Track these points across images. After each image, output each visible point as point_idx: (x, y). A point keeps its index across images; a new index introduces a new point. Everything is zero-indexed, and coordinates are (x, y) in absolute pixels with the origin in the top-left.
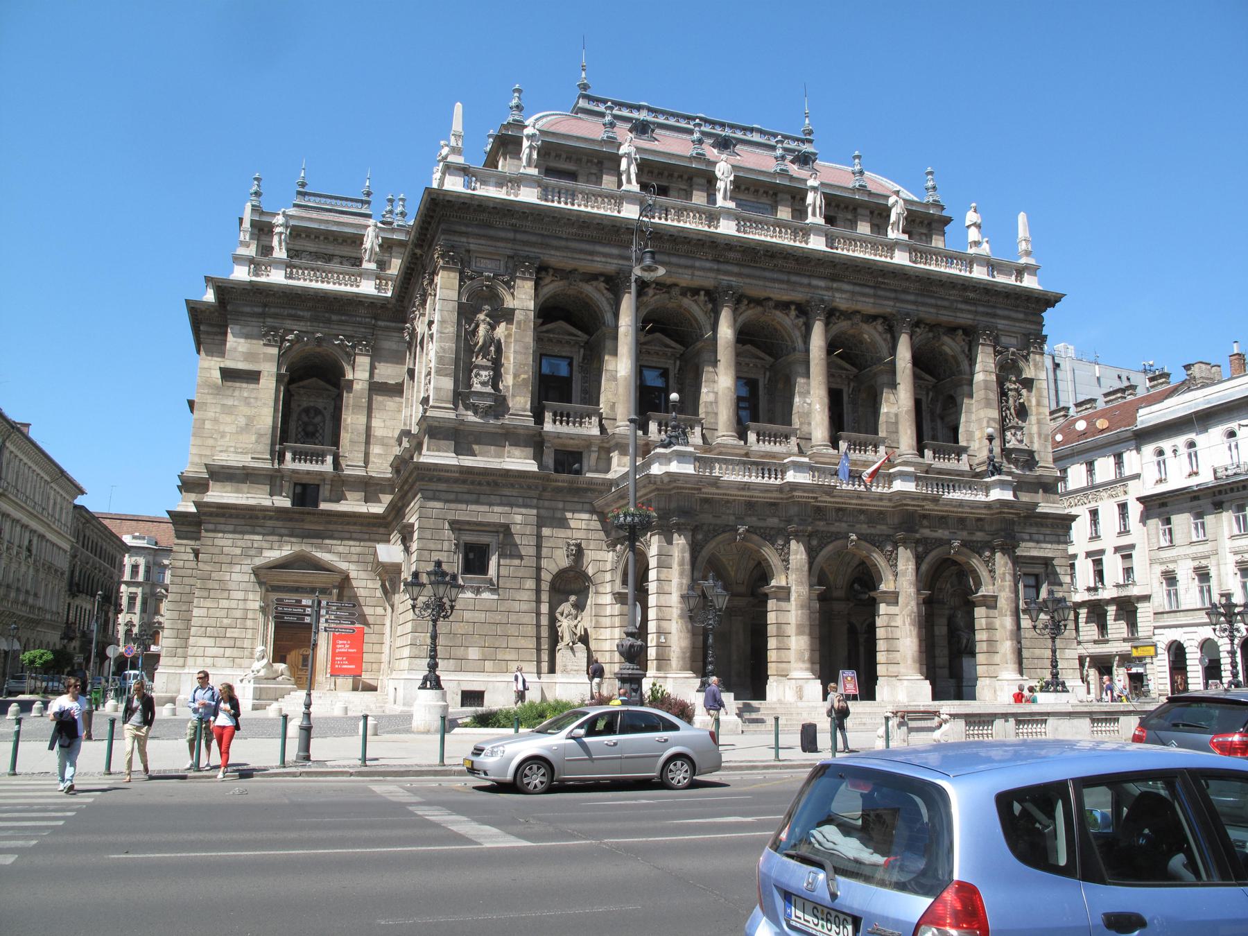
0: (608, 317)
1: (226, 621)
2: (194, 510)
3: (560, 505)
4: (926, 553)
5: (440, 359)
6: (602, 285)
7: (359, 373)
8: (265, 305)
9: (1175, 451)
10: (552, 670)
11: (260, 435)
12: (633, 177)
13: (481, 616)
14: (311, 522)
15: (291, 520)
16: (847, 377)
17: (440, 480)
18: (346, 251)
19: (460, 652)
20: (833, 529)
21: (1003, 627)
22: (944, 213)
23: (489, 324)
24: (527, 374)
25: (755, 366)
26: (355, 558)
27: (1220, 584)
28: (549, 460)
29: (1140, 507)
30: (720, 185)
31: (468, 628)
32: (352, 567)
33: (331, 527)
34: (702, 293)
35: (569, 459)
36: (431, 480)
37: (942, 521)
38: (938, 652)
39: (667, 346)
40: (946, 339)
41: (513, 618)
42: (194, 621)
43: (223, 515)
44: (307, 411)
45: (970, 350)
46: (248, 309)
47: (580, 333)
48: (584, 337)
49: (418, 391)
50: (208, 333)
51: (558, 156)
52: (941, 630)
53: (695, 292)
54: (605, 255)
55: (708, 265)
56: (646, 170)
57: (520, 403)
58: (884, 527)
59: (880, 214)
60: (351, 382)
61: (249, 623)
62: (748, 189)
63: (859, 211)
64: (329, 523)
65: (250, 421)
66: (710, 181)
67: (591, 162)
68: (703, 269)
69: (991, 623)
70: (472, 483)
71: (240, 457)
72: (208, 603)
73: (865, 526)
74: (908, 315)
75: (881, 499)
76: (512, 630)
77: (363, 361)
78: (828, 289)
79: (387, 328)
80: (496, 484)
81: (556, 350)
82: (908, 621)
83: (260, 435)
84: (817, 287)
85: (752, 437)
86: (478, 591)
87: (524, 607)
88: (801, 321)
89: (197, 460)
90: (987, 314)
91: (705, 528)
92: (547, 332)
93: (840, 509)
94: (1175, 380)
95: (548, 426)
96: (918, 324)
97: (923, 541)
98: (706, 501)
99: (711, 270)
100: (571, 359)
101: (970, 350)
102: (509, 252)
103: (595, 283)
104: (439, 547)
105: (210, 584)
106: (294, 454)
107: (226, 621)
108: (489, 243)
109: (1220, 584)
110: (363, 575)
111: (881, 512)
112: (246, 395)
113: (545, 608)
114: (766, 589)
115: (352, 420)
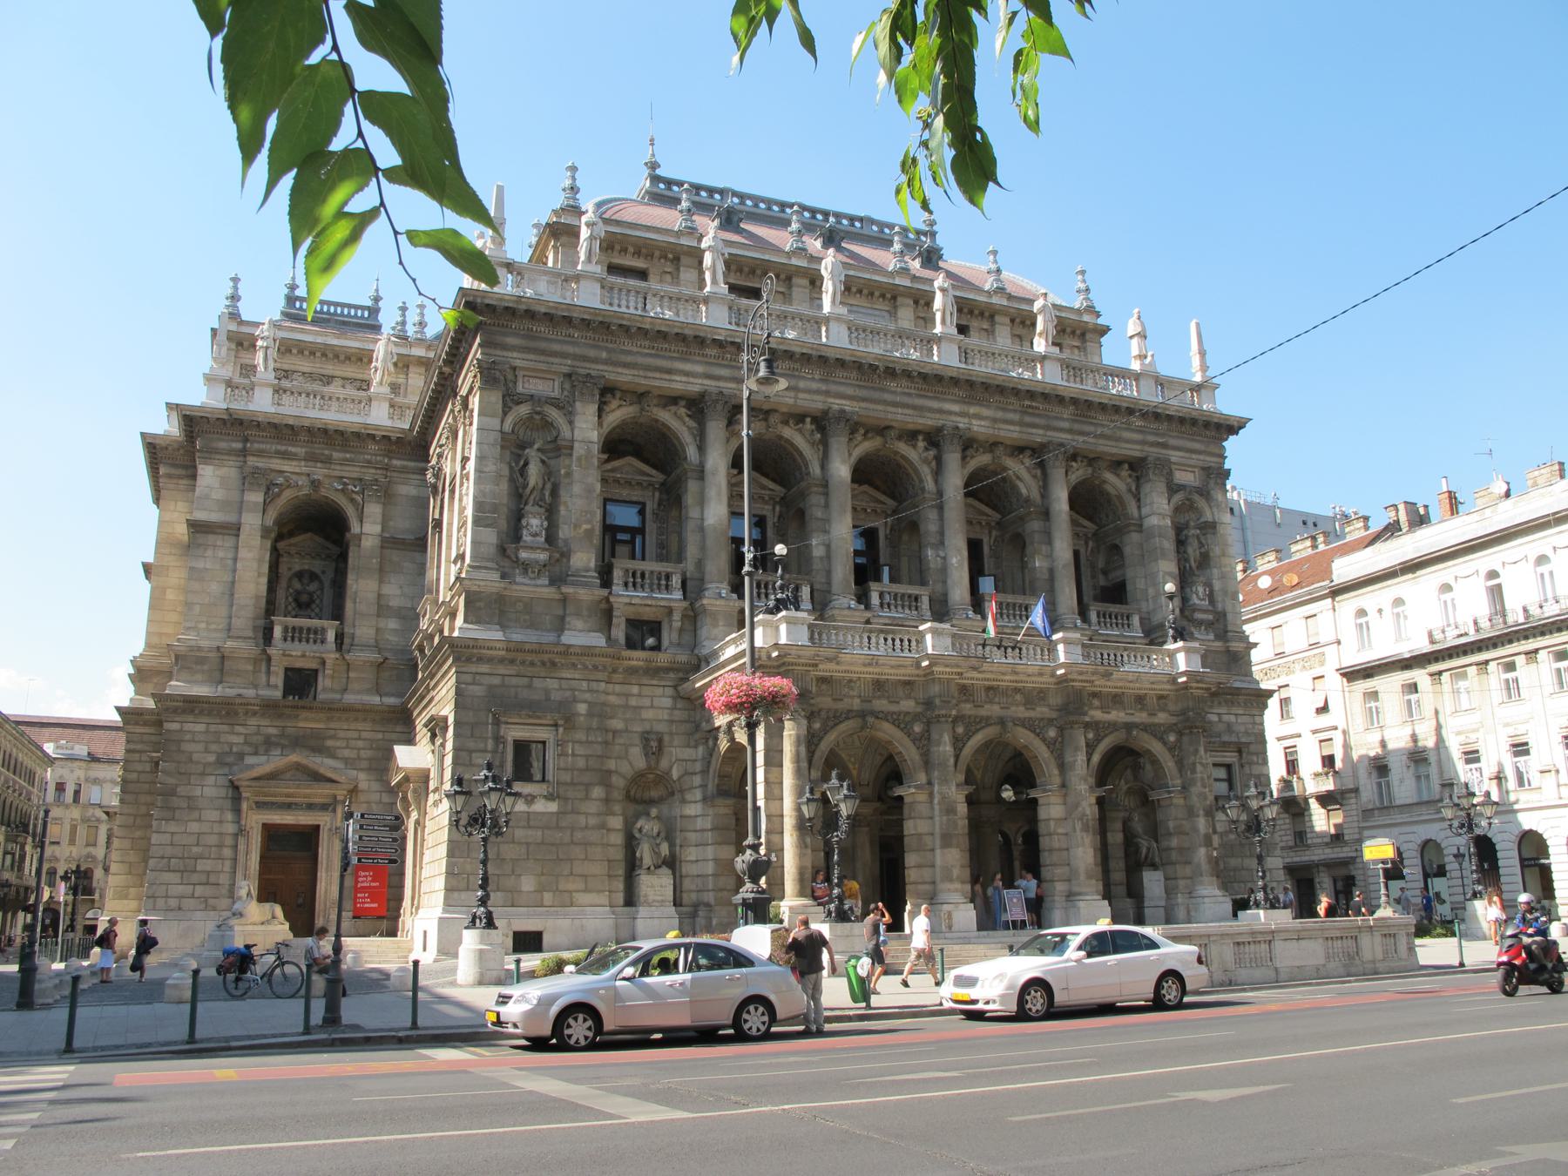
0: (691, 452)
2: (150, 704)
3: (635, 690)
4: (1098, 740)
5: (479, 506)
6: (683, 411)
7: (368, 528)
8: (246, 440)
9: (1380, 611)
12: (720, 277)
14: (306, 719)
15: (280, 716)
16: (988, 524)
17: (480, 659)
18: (350, 371)
20: (983, 712)
21: (1195, 830)
22: (1100, 321)
23: (543, 462)
25: (874, 511)
26: (365, 764)
27: (1441, 773)
28: (619, 633)
30: (828, 286)
32: (362, 776)
33: (332, 725)
34: (808, 420)
35: (643, 631)
36: (469, 660)
37: (1116, 700)
38: (1112, 864)
39: (764, 487)
40: (1109, 476)
41: (578, 835)
42: (154, 851)
43: (192, 711)
44: (300, 575)
45: (1138, 487)
46: (223, 445)
47: (654, 472)
48: (659, 477)
49: (449, 548)
50: (170, 476)
51: (624, 250)
52: (1116, 838)
53: (800, 418)
54: (687, 374)
55: (814, 386)
56: (733, 267)
57: (584, 559)
58: (1045, 709)
59: (1023, 323)
60: (359, 537)
62: (860, 292)
63: (997, 318)
64: (329, 719)
66: (815, 281)
67: (666, 257)
68: (809, 391)
70: (523, 663)
72: (172, 827)
73: (1022, 708)
74: (1062, 445)
75: (1041, 674)
76: (577, 851)
77: (374, 510)
78: (963, 414)
79: (404, 470)
80: (554, 664)
81: (625, 493)
84: (950, 413)
86: (530, 799)
87: (592, 821)
88: (932, 453)
89: (155, 640)
90: (1158, 444)
91: (823, 714)
92: (612, 470)
93: (989, 689)
94: (1376, 526)
96: (1074, 457)
97: (1094, 725)
98: (823, 680)
99: (818, 392)
100: (643, 505)
102: (566, 370)
103: (673, 408)
105: (175, 802)
106: (286, 630)
107: (195, 849)
108: (542, 358)
109: (1441, 773)
110: (376, 786)
111: (1041, 691)
112: (221, 554)
113: (616, 822)
115: (362, 588)
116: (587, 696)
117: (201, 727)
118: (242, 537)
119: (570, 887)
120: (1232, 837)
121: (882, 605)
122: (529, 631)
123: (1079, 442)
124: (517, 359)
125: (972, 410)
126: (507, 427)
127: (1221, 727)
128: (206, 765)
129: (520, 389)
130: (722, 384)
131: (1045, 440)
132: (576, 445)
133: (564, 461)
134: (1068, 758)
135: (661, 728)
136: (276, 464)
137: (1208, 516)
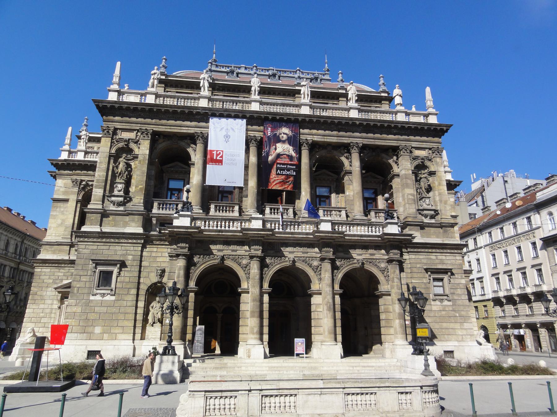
1: (41, 315)
3: (155, 250)
10: (143, 338)
11: (66, 228)
12: (206, 89)
13: (104, 309)
19: (90, 329)
21: (394, 311)
23: (125, 163)
24: (142, 186)
29: (541, 242)
30: (253, 89)
31: (97, 316)
41: (122, 310)
45: (397, 159)
61: (53, 315)
65: (63, 221)
69: (388, 308)
71: (57, 238)
76: (121, 316)
82: (325, 307)
83: (66, 228)
85: (267, 210)
86: (103, 295)
87: (129, 304)
95: (155, 211)
101: (397, 159)
102: (138, 128)
104: (86, 274)
107: (41, 315)
112: (62, 210)
113: (141, 304)
114: (377, 293)
116: (133, 253)
117: (48, 270)
118: (70, 203)
119: (117, 331)
120: (444, 313)
121: (271, 213)
122: (113, 228)
123: (366, 142)
124: (118, 126)
125: (314, 131)
126: (113, 151)
127: (437, 261)
128: (48, 284)
129: (120, 137)
130: (202, 129)
131: (349, 142)
132: (139, 156)
133: (137, 162)
134: (322, 276)
135: (164, 265)
136: (83, 178)
137: (432, 169)
